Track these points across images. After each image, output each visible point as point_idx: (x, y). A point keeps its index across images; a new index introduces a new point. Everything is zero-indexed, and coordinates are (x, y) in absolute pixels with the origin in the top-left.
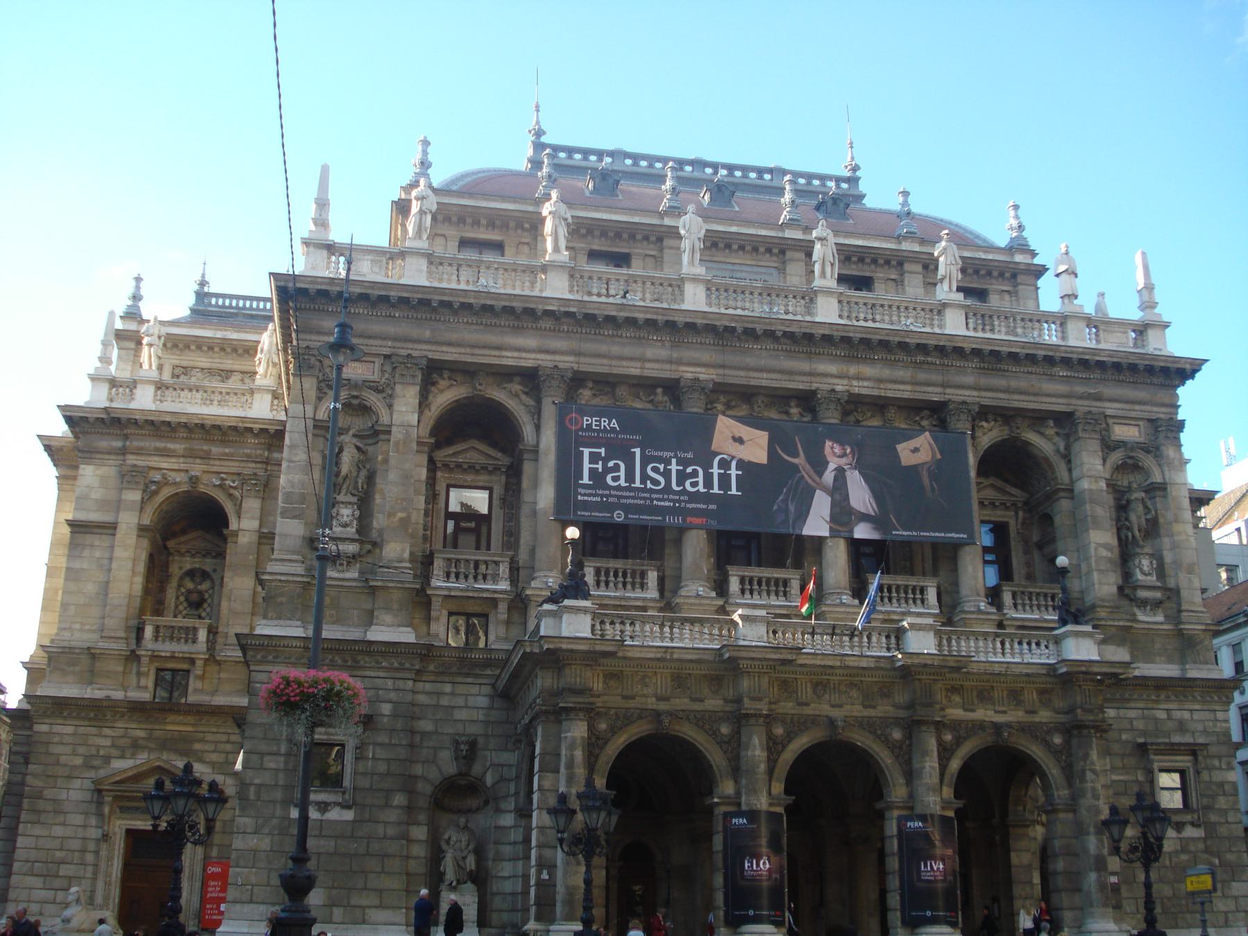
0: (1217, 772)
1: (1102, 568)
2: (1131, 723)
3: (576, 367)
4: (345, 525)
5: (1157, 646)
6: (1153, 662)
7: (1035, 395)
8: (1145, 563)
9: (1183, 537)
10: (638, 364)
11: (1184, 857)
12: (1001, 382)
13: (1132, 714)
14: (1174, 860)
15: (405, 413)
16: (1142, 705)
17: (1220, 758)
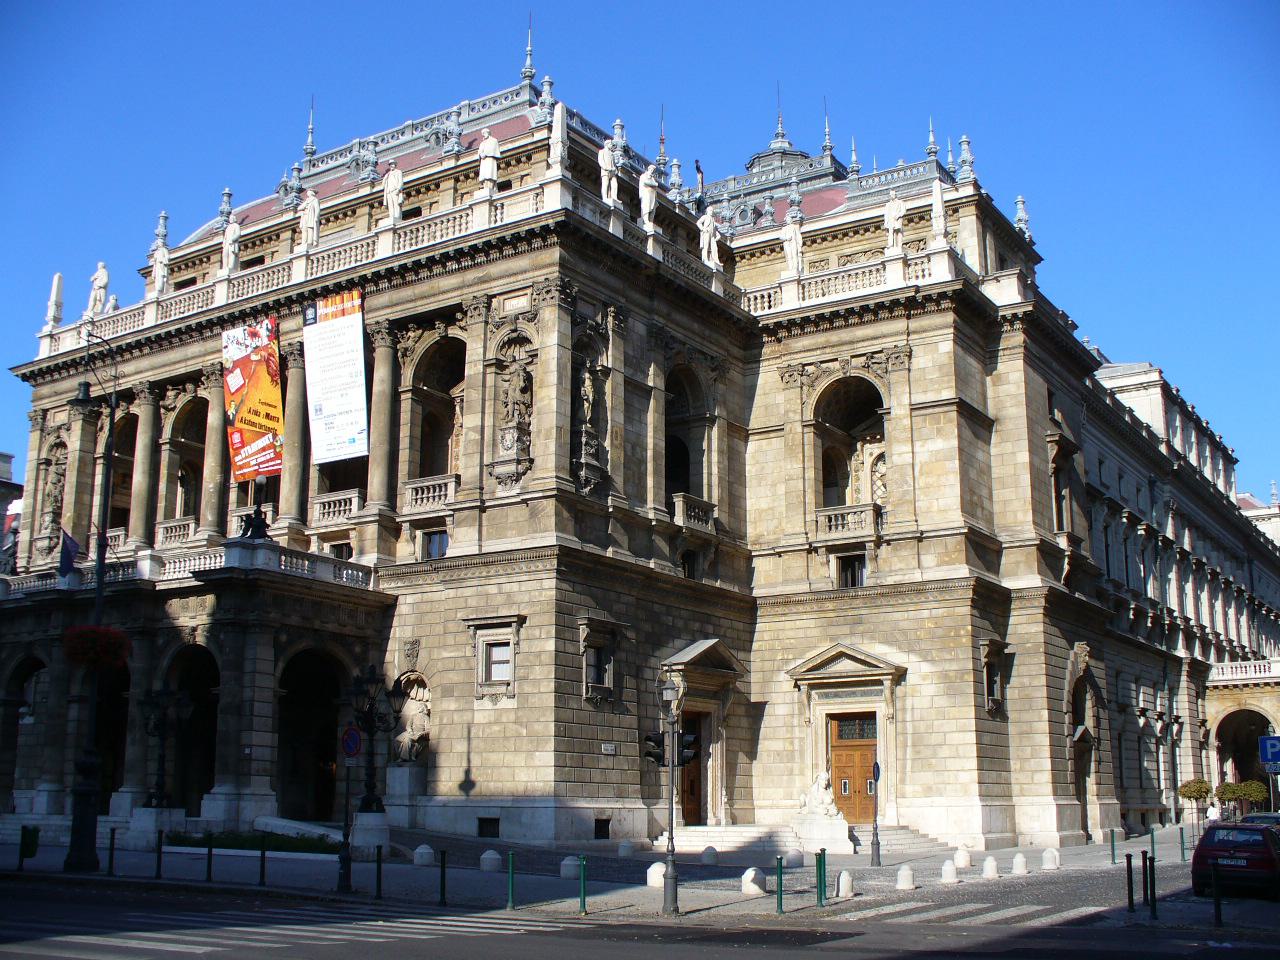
0: (536, 642)
1: (469, 451)
2: (466, 602)
3: (152, 379)
4: (46, 529)
5: (511, 520)
6: (506, 537)
7: (434, 295)
8: (509, 437)
9: (545, 403)
10: (183, 364)
11: (496, 728)
12: (407, 292)
13: (468, 592)
14: (488, 731)
15: (74, 441)
16: (475, 582)
17: (540, 626)
